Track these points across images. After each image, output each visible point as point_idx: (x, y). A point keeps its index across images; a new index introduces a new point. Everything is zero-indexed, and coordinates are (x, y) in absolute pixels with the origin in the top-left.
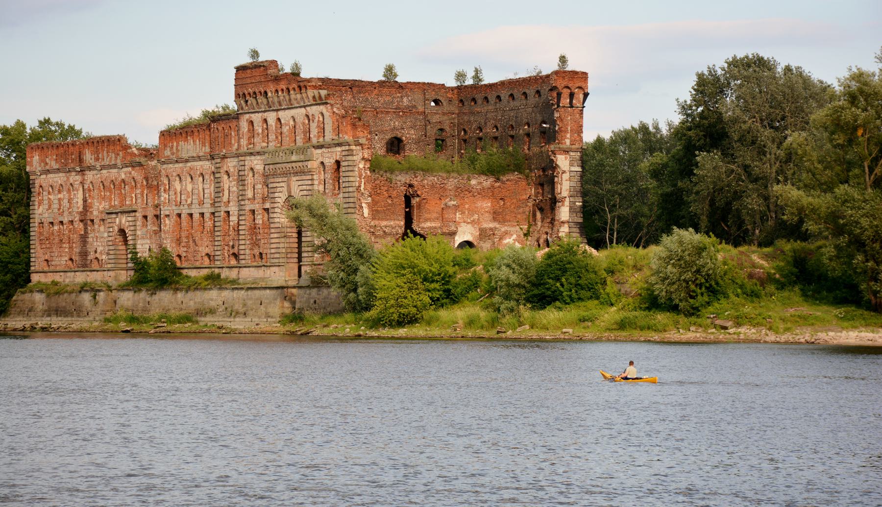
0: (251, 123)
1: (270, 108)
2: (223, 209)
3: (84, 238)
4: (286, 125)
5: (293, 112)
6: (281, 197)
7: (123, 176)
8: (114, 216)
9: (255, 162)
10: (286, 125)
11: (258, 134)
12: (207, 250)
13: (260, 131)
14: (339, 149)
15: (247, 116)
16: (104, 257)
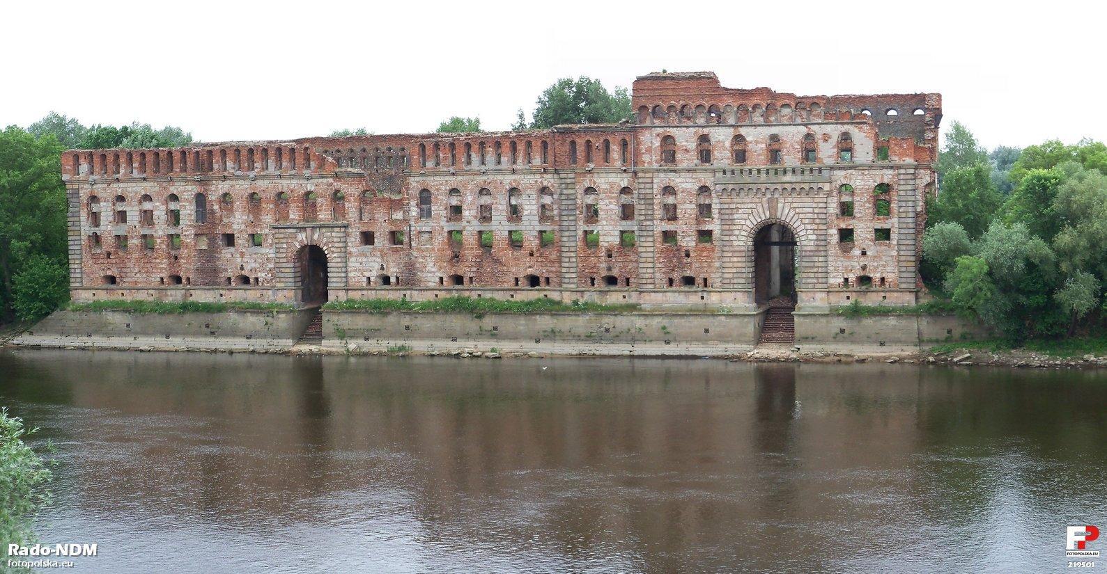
0: (667, 140)
1: (720, 121)
2: (582, 227)
3: (209, 256)
4: (757, 142)
5: (774, 130)
6: (748, 217)
7: (310, 187)
8: (294, 231)
9: (678, 180)
10: (757, 142)
11: (687, 151)
12: (530, 271)
13: (692, 145)
14: (890, 172)
15: (659, 130)
16: (261, 275)
